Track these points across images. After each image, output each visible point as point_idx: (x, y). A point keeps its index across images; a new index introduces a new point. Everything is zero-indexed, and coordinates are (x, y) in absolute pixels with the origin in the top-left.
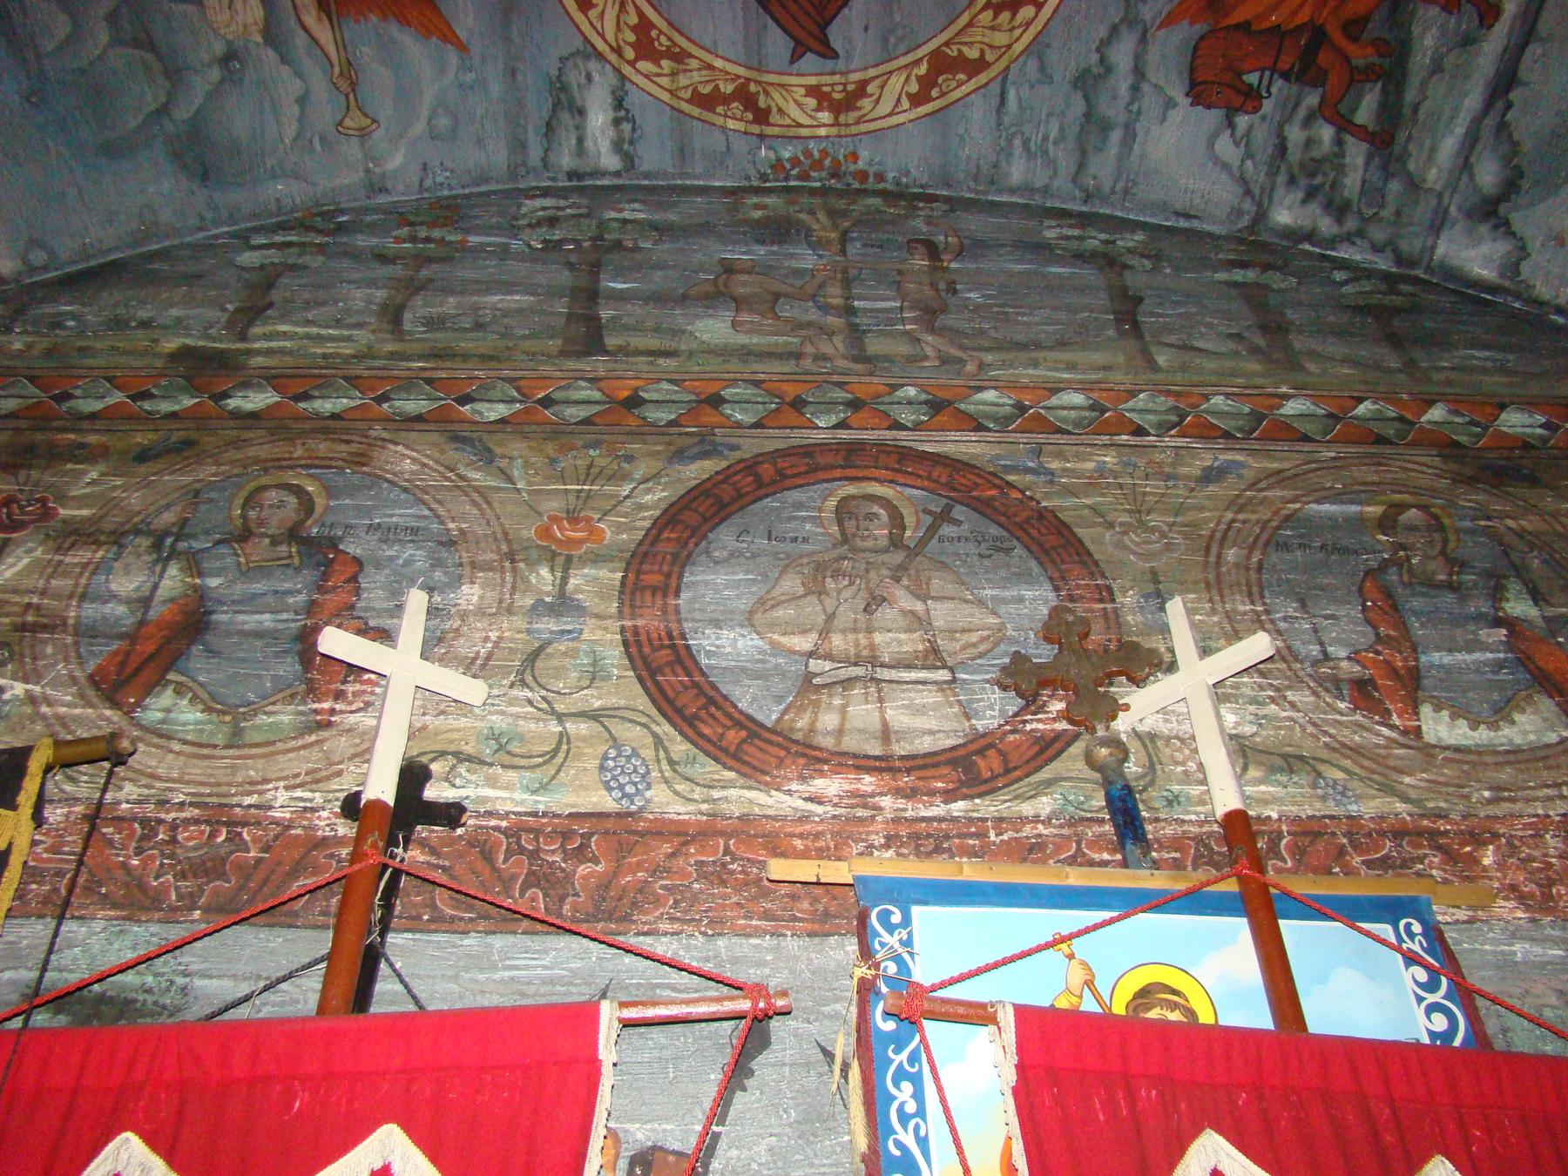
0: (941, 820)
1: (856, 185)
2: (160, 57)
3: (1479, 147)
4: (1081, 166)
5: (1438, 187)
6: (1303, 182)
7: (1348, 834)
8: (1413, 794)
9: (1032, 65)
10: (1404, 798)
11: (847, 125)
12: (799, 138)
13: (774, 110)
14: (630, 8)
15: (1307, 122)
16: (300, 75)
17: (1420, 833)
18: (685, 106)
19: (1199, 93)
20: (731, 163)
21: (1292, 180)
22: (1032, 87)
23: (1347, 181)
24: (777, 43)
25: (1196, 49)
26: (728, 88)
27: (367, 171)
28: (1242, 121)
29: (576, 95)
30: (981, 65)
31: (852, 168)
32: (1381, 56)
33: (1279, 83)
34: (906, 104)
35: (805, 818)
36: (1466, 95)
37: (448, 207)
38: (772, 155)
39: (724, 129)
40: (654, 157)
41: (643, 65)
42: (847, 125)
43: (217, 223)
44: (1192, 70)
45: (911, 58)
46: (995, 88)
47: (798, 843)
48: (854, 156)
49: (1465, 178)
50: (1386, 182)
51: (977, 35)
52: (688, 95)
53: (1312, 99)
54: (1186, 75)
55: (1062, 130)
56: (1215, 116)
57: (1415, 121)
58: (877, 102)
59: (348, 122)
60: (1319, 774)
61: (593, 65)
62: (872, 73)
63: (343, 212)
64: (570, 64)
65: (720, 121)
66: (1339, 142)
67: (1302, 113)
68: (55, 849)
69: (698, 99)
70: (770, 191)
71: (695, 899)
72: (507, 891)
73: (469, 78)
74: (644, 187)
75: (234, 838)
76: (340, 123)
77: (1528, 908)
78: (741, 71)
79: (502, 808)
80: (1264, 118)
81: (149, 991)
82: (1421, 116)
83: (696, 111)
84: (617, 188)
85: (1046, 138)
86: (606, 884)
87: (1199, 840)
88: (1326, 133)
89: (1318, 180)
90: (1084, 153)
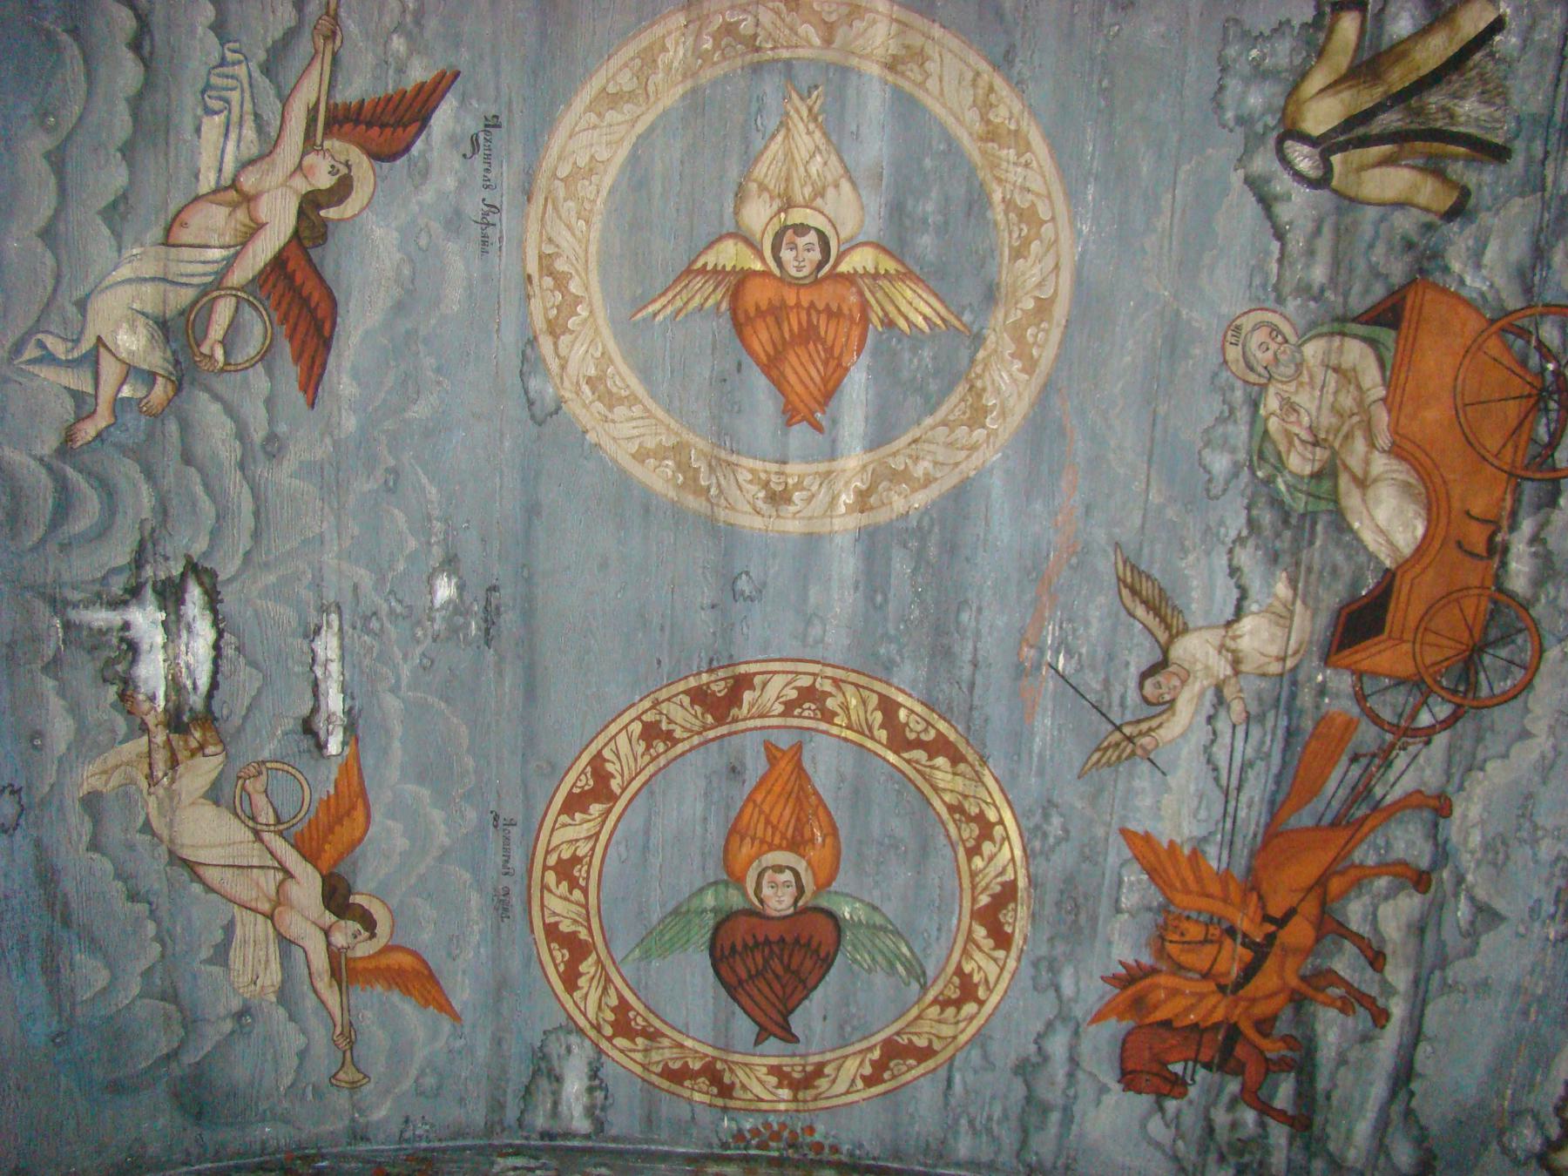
1: (811, 1155)
2: (181, 1010)
3: (1390, 1130)
4: (1024, 1143)
5: (1359, 1166)
6: (1232, 1160)
9: (975, 1054)
11: (805, 1101)
12: (758, 1111)
13: (738, 1085)
14: (612, 991)
15: (1232, 1105)
16: (304, 1031)
18: (654, 1078)
19: (1129, 1079)
20: (694, 1131)
21: (1222, 1159)
22: (976, 1072)
23: (1274, 1160)
24: (744, 1027)
25: (1124, 1041)
26: (696, 1065)
27: (353, 1120)
28: (1171, 1105)
29: (555, 1063)
30: (926, 1053)
31: (809, 1139)
32: (1291, 1049)
33: (1201, 1073)
34: (860, 1084)
36: (1371, 1084)
37: (424, 1159)
38: (734, 1126)
39: (690, 1101)
40: (623, 1122)
41: (621, 1042)
42: (805, 1101)
43: (199, 1160)
44: (1122, 1060)
45: (865, 1044)
46: (942, 1073)
48: (811, 1130)
49: (1382, 1159)
50: (1309, 1161)
51: (925, 1026)
52: (658, 1069)
53: (1233, 1086)
54: (1117, 1065)
55: (1005, 1110)
56: (1144, 1101)
57: (1330, 1107)
58: (834, 1081)
59: (341, 1075)
61: (574, 1039)
62: (829, 1056)
63: (323, 1157)
64: (553, 1037)
65: (687, 1093)
66: (1262, 1125)
67: (1225, 1099)
69: (668, 1074)
70: (729, 1159)
73: (459, 1043)
74: (612, 1151)
76: (334, 1076)
78: (710, 1051)
80: (1191, 1102)
82: (1334, 1102)
83: (665, 1084)
84: (583, 1150)
85: (990, 1118)
88: (1249, 1116)
89: (1247, 1158)
90: (1025, 1131)
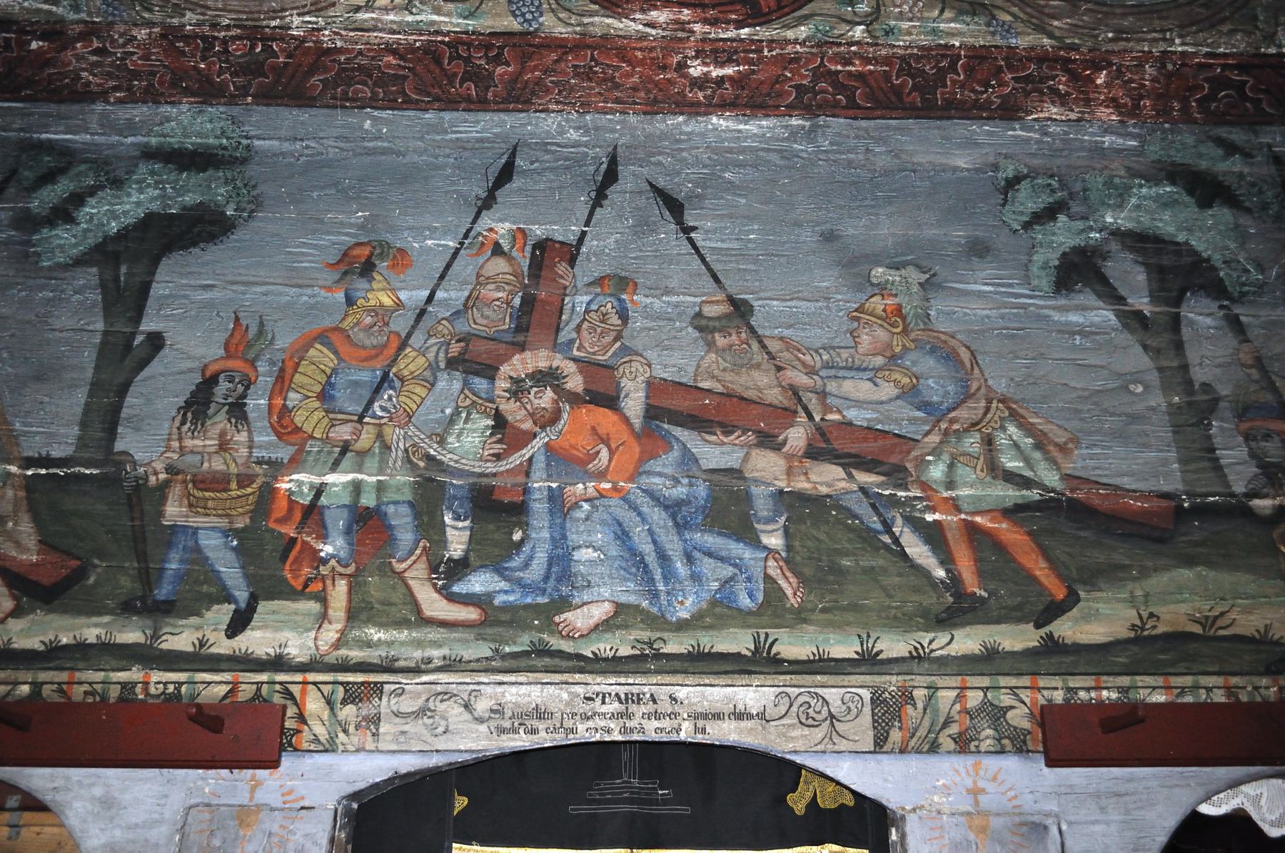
0: (732, 40)
7: (1006, 59)
8: (1057, 33)
10: (1051, 36)
17: (1056, 59)
35: (644, 37)
47: (639, 54)
60: (994, 17)
68: (146, 57)
71: (572, 89)
72: (451, 83)
75: (267, 49)
77: (1120, 114)
79: (445, 29)
81: (225, 148)
86: (515, 78)
87: (903, 58)
